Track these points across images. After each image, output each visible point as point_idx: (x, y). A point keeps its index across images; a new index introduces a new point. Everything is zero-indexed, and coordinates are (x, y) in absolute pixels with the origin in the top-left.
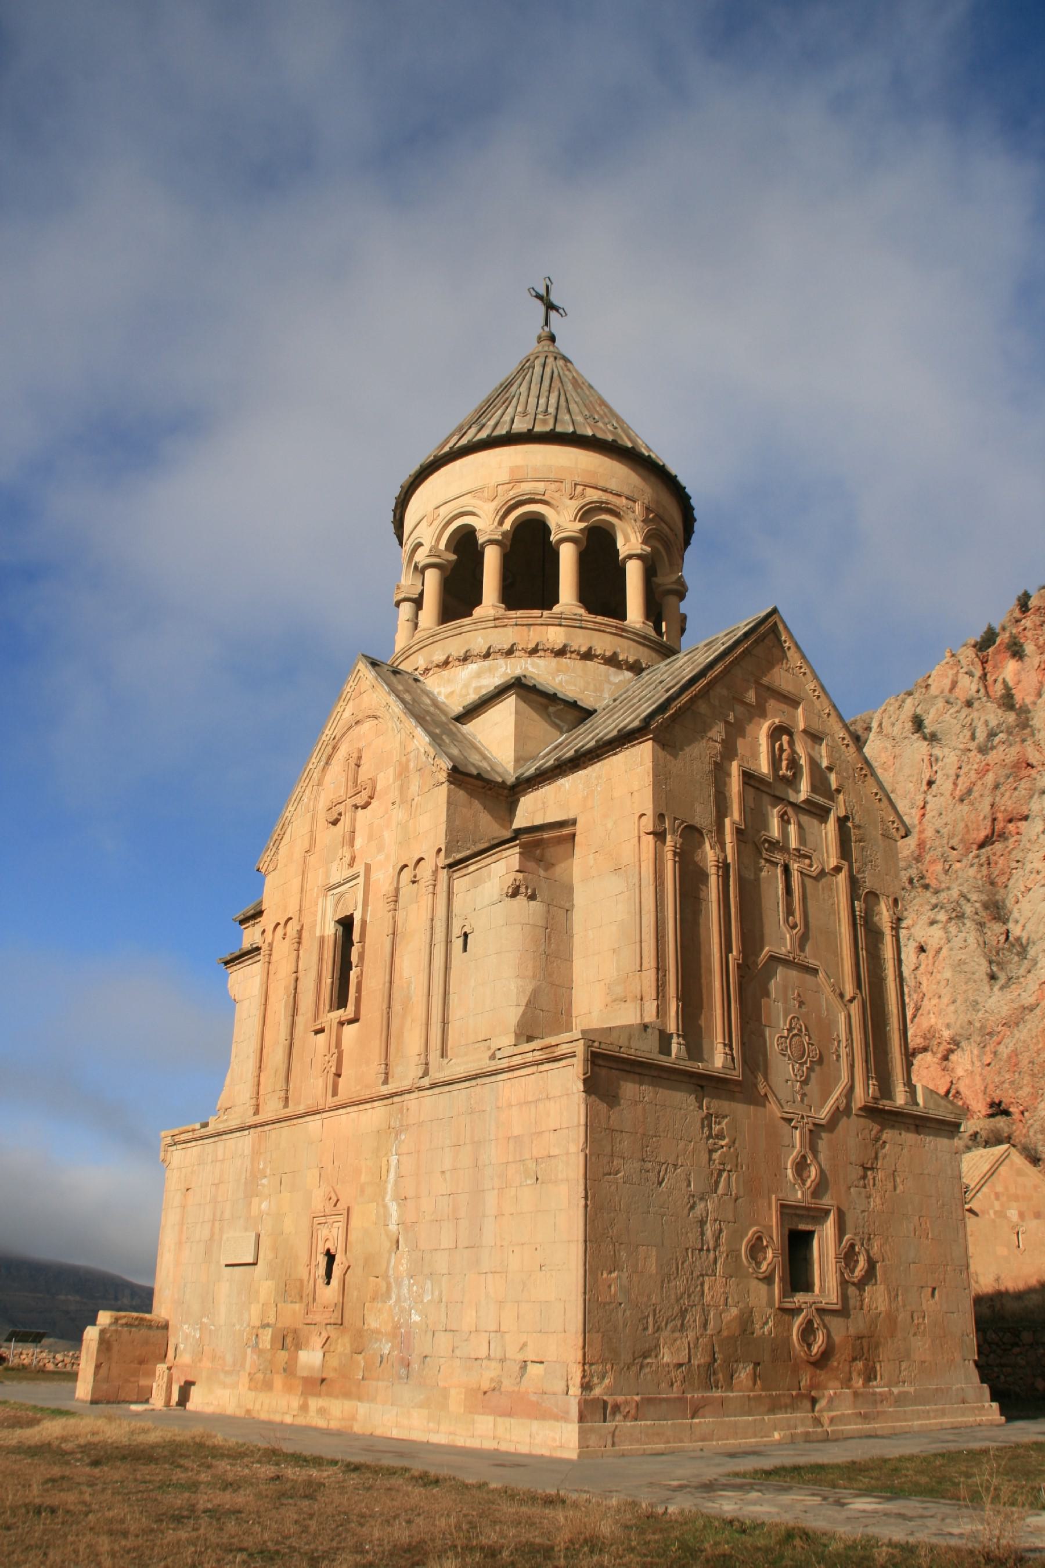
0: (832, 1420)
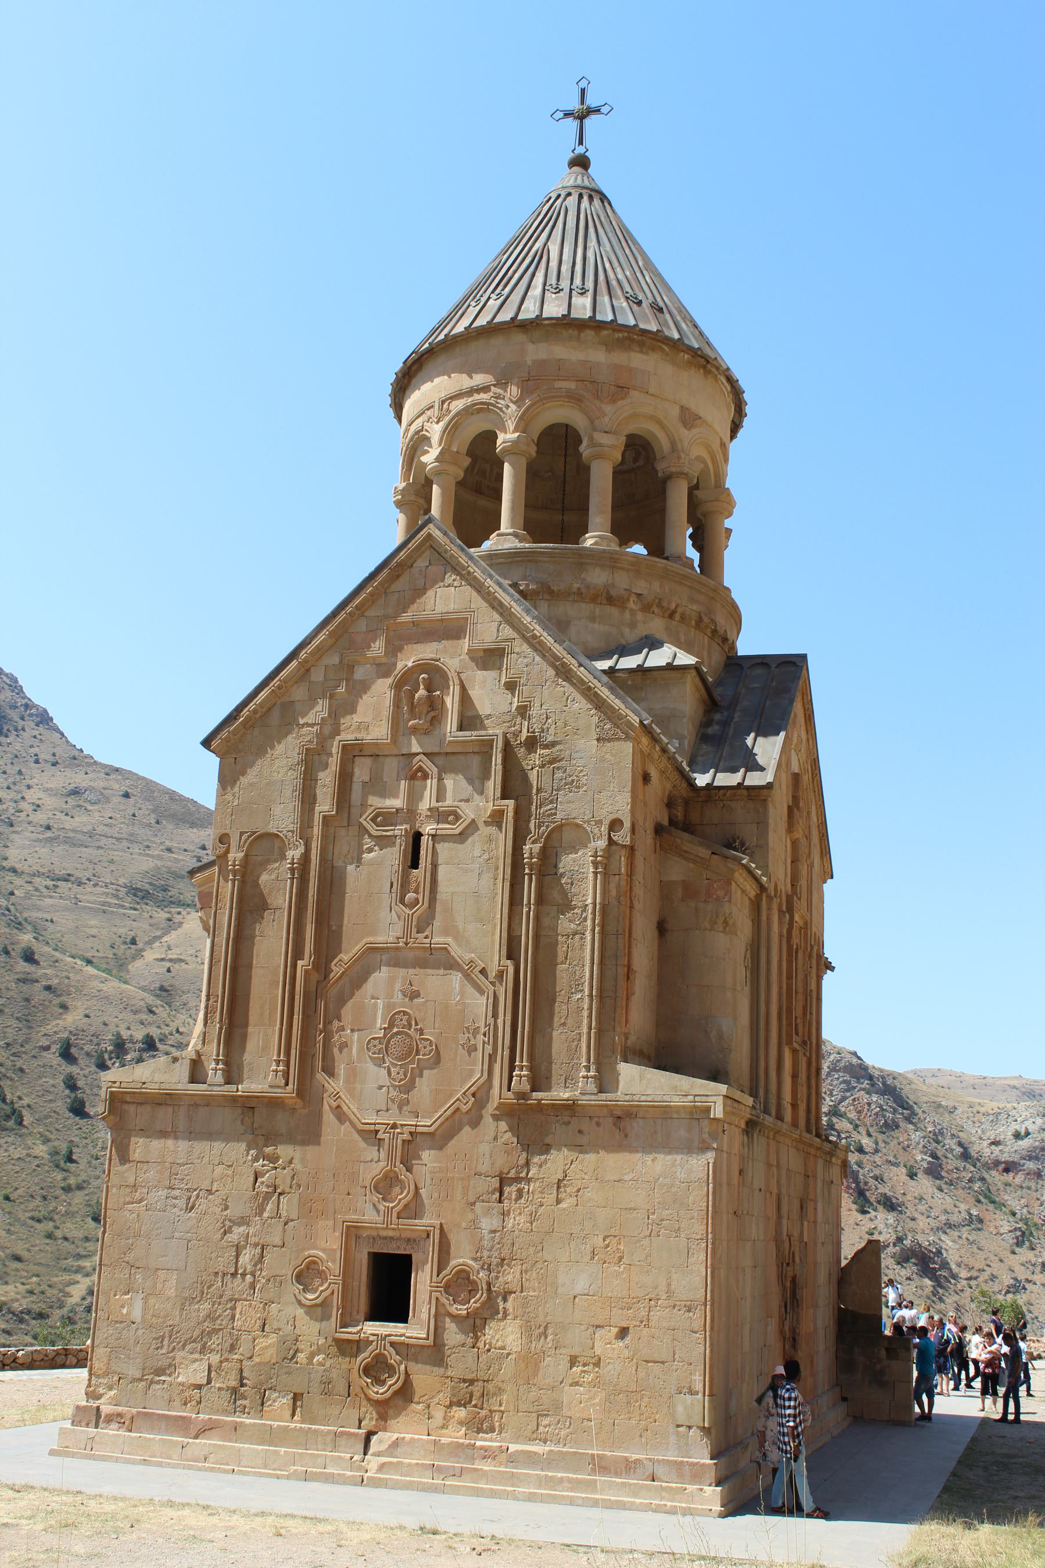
0: (382, 1467)
